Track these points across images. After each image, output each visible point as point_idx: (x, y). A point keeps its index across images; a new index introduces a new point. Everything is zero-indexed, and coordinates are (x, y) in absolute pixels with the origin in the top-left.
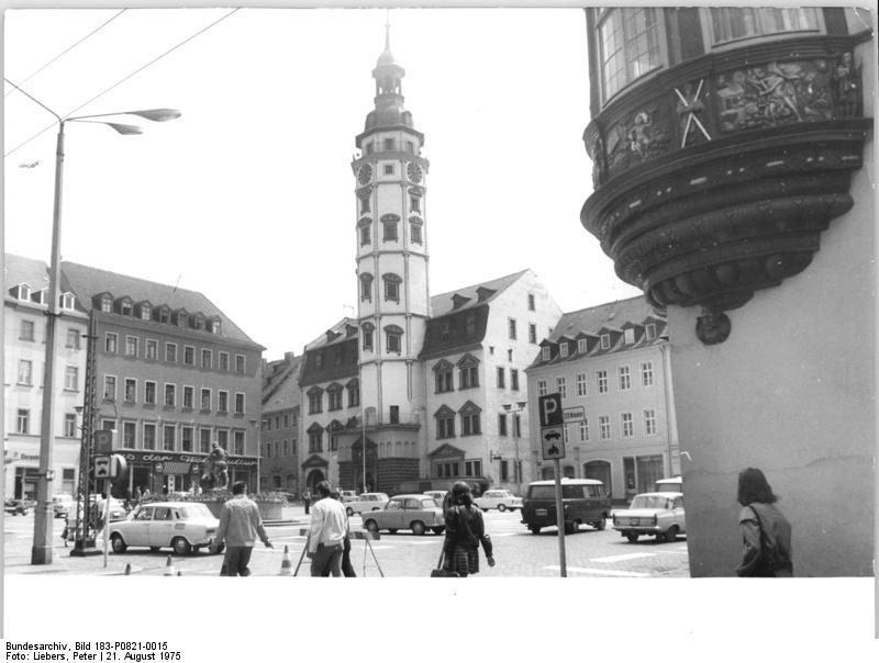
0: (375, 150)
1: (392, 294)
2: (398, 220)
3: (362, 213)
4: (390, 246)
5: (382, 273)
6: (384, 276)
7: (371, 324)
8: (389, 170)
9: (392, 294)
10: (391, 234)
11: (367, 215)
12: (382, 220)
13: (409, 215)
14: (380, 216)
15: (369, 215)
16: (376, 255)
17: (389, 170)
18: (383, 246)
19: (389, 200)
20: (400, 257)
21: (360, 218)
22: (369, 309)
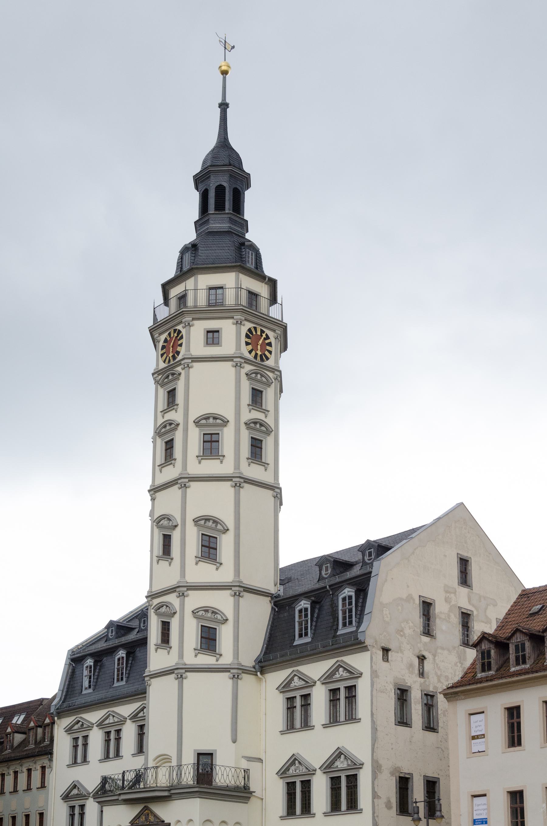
0: (190, 302)
1: (209, 550)
2: (226, 423)
3: (164, 412)
4: (211, 467)
5: (192, 513)
6: (196, 521)
7: (167, 605)
8: (213, 337)
9: (209, 550)
10: (211, 446)
11: (171, 416)
12: (197, 423)
13: (248, 415)
14: (193, 417)
15: (175, 416)
16: (183, 482)
17: (213, 337)
18: (196, 468)
19: (213, 388)
20: (227, 487)
21: (160, 421)
22: (170, 576)
